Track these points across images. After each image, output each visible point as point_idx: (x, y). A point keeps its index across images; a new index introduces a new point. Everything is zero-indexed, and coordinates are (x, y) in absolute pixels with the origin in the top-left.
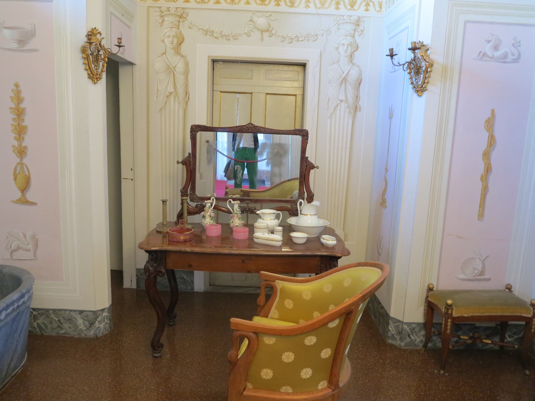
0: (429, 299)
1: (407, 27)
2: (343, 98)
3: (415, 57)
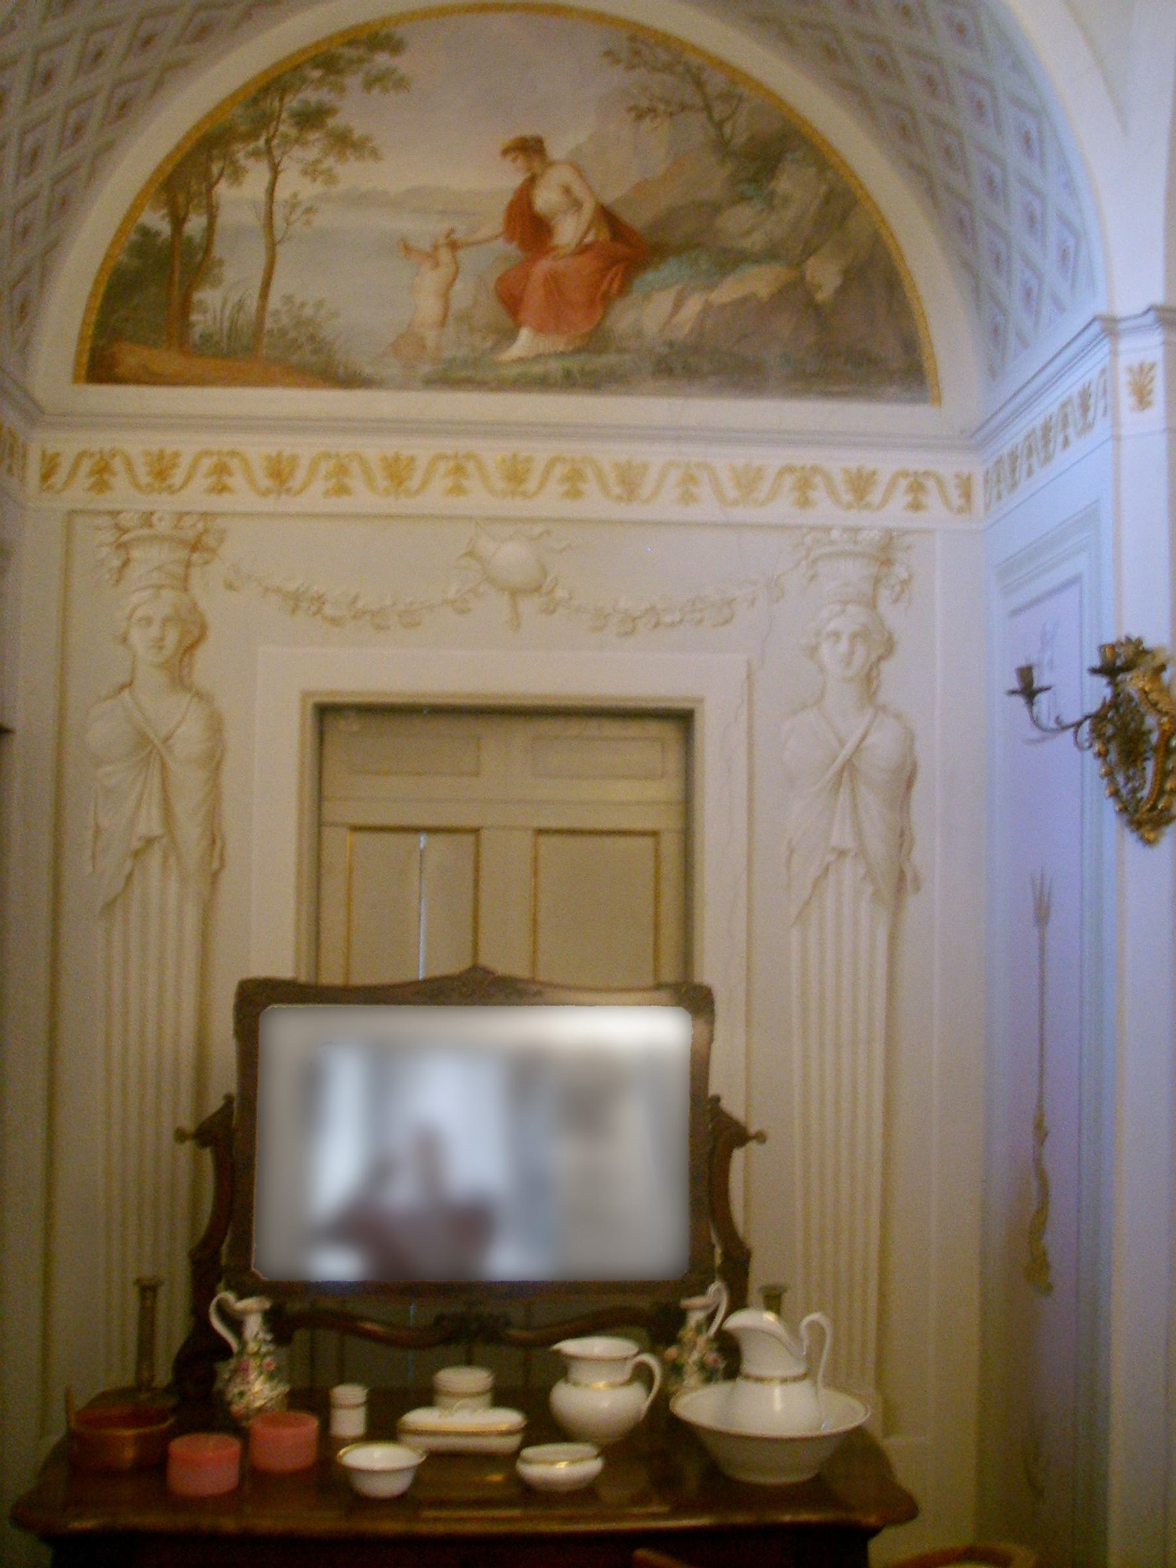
1: (1075, 580)
2: (849, 843)
3: (1116, 695)
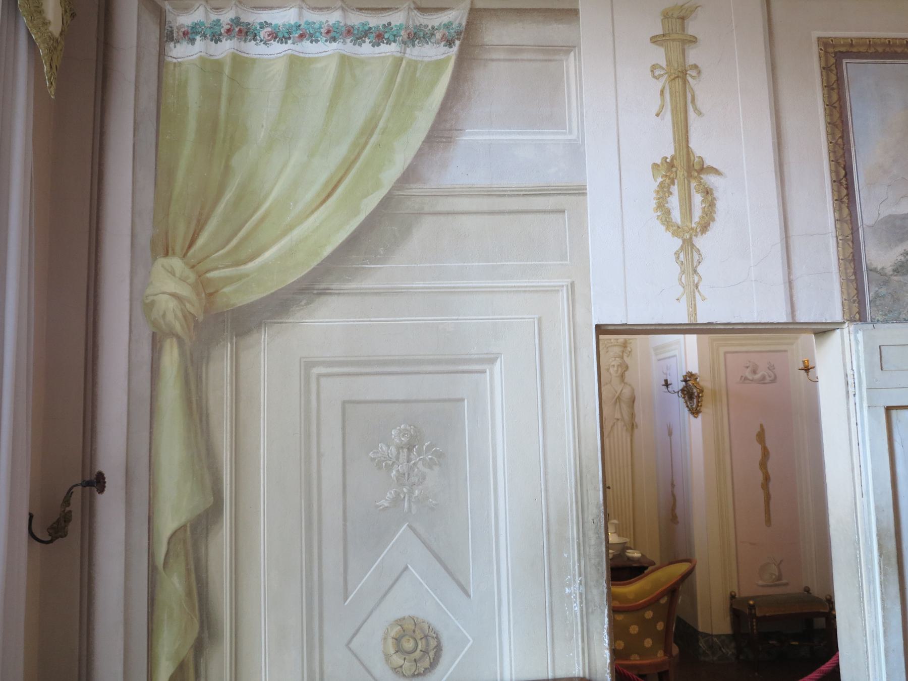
0: (734, 607)
1: (675, 356)
2: (619, 416)
